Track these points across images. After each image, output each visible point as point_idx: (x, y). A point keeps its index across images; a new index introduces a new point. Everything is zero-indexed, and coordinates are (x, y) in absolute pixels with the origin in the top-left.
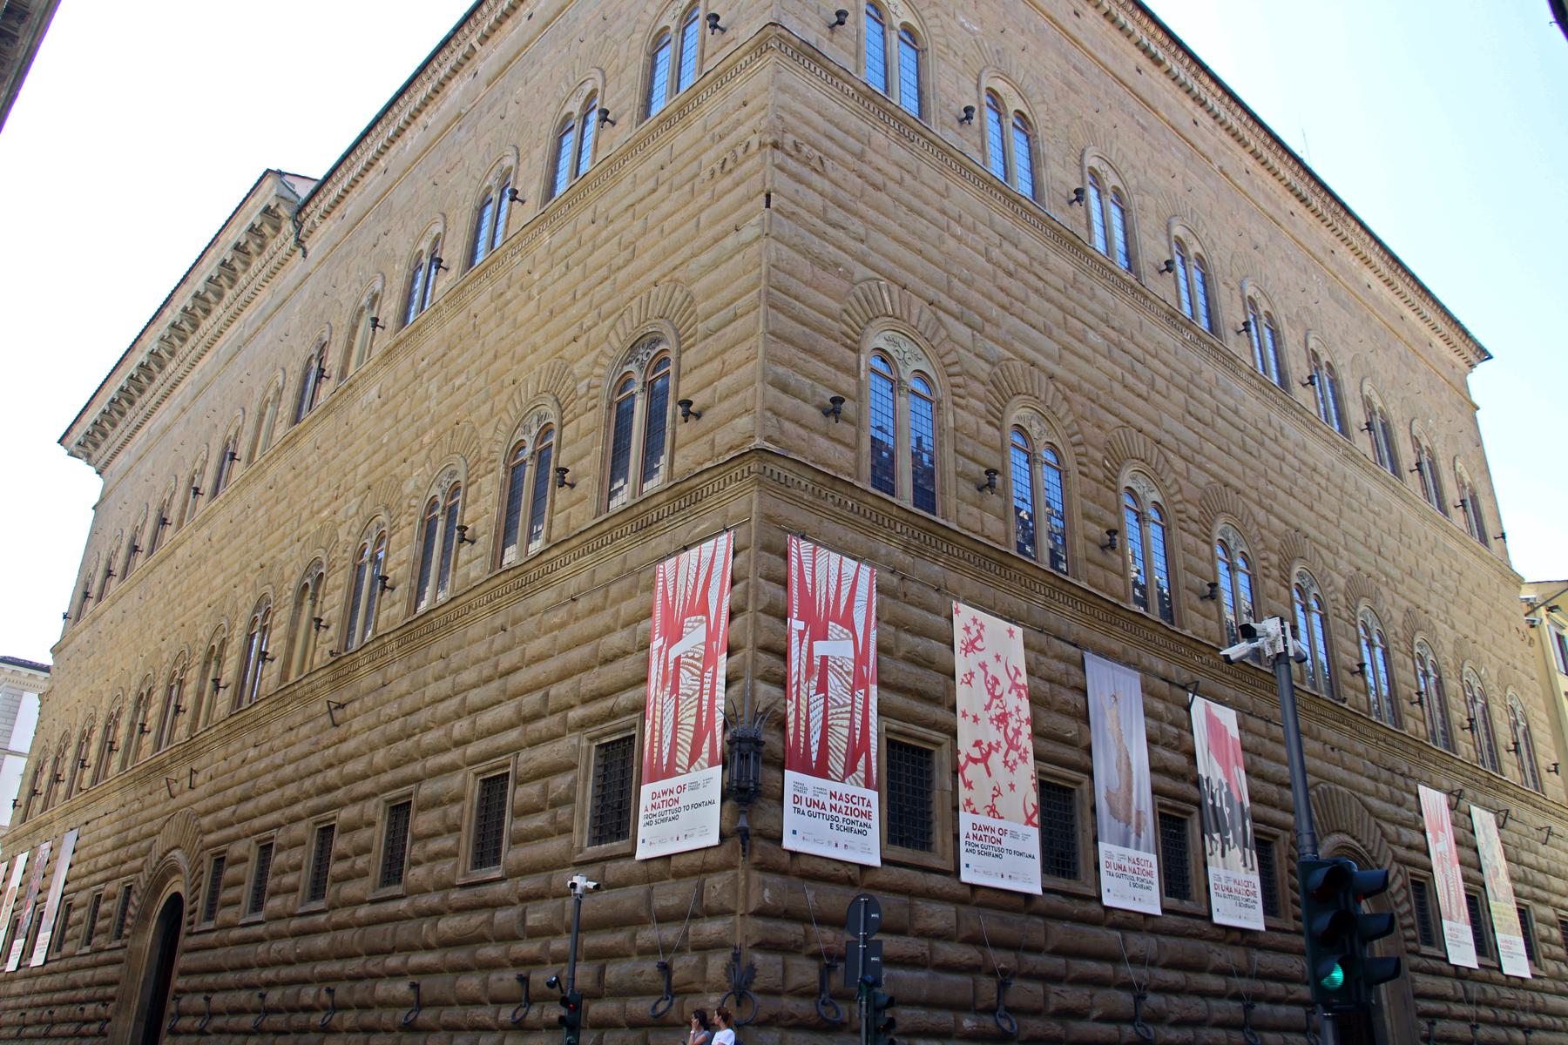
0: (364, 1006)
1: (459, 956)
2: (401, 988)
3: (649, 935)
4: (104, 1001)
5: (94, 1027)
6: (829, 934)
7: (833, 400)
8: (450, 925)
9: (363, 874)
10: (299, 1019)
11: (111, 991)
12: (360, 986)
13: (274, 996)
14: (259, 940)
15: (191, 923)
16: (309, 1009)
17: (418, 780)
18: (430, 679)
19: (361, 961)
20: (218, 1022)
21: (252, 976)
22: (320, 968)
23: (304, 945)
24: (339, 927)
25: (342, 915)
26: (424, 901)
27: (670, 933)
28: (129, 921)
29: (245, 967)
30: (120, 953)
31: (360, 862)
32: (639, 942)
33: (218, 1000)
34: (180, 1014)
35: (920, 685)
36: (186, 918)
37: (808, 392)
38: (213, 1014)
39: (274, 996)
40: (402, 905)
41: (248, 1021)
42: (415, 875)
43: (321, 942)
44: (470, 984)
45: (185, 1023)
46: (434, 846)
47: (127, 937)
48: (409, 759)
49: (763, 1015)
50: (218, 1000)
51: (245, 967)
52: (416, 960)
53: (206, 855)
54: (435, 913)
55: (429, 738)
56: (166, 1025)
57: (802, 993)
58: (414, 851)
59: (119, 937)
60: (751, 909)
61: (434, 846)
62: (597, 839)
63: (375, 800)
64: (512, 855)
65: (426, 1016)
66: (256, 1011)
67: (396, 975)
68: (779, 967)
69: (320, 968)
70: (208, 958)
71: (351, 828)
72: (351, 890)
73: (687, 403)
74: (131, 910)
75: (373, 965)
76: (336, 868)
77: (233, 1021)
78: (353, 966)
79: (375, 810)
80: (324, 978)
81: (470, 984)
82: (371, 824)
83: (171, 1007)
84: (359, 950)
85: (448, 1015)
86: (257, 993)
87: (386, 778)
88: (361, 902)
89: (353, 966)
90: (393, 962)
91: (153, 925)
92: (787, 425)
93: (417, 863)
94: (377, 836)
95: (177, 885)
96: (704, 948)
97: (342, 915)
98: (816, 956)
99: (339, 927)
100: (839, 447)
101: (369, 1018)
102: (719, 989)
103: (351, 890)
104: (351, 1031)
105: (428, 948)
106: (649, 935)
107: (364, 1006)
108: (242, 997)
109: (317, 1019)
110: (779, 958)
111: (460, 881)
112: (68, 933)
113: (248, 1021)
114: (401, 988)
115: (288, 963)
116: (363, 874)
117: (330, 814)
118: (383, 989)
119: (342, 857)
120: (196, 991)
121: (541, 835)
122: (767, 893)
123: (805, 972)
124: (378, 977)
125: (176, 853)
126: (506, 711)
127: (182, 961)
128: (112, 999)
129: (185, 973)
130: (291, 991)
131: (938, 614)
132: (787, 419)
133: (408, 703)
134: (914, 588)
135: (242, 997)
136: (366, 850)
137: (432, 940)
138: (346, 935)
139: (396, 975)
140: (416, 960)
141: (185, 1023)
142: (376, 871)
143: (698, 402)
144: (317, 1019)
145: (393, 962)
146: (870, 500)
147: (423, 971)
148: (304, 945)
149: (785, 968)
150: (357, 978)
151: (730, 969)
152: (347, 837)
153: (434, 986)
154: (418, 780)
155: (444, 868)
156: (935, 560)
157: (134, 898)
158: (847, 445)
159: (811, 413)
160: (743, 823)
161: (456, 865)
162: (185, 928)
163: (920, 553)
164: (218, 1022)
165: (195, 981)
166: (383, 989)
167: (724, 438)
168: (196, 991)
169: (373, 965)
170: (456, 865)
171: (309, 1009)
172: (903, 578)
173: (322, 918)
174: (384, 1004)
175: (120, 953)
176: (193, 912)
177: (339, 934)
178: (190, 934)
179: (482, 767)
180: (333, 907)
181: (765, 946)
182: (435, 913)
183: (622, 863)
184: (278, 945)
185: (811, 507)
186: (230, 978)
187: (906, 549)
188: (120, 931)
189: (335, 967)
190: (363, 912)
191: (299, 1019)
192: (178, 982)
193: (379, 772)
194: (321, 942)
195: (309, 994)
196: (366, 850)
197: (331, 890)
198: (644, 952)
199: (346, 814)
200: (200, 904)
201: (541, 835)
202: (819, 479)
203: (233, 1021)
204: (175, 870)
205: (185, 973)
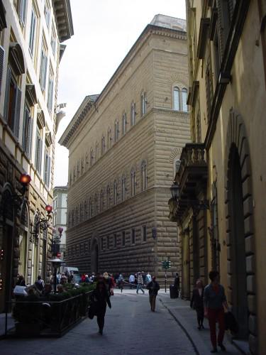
1: (131, 256)
13: (112, 262)
29: (107, 258)
42: (126, 244)
44: (133, 260)
54: (128, 250)
65: (129, 265)
70: (103, 256)
78: (121, 258)
90: (125, 257)
103: (119, 246)
114: (125, 261)
127: (100, 256)
136: (120, 240)
147: (128, 259)
192: (99, 260)
195: (116, 262)
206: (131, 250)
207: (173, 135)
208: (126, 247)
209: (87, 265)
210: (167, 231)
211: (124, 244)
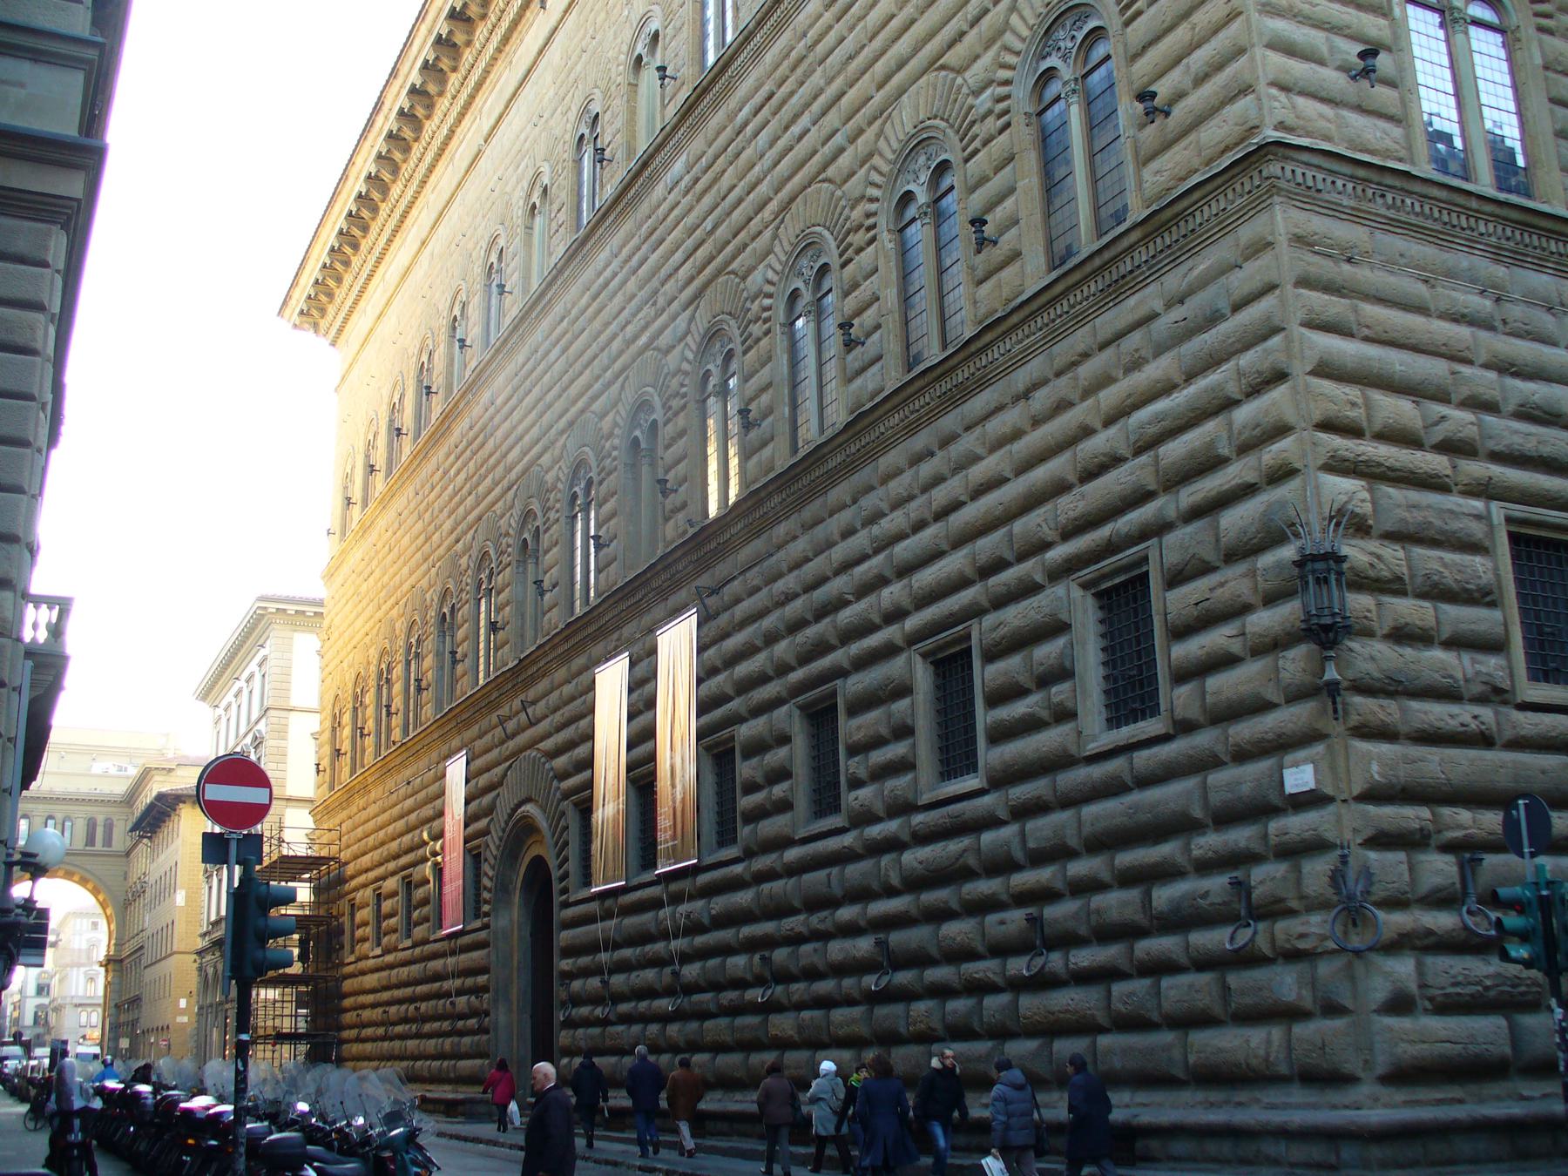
2: (864, 946)
3: (1209, 842)
6: (1464, 815)
7: (1363, 55)
8: (914, 858)
9: (784, 806)
11: (482, 979)
12: (806, 948)
15: (565, 891)
16: (740, 984)
17: (840, 673)
18: (836, 537)
19: (802, 917)
22: (747, 931)
23: (719, 904)
25: (763, 863)
26: (875, 831)
27: (1241, 836)
28: (486, 895)
30: (483, 935)
31: (779, 790)
32: (1196, 853)
35: (1546, 450)
36: (556, 887)
37: (1324, 50)
39: (691, 971)
40: (847, 840)
43: (743, 898)
44: (957, 930)
46: (879, 756)
47: (487, 914)
48: (821, 648)
49: (1387, 934)
52: (879, 908)
54: (893, 845)
55: (846, 616)
56: (560, 1016)
57: (1441, 900)
58: (850, 766)
59: (477, 916)
60: (1355, 793)
61: (879, 756)
62: (1114, 722)
63: (785, 708)
64: (990, 756)
67: (851, 930)
68: (1405, 867)
71: (756, 748)
72: (771, 827)
73: (1145, 96)
74: (486, 882)
75: (816, 920)
79: (787, 717)
81: (957, 930)
84: (797, 904)
86: (668, 970)
87: (796, 676)
90: (846, 913)
91: (517, 898)
92: (1301, 102)
93: (856, 784)
94: (797, 753)
96: (1294, 851)
97: (763, 863)
98: (1448, 848)
100: (1382, 124)
101: (825, 987)
102: (1323, 905)
103: (771, 827)
106: (1209, 842)
107: (812, 974)
108: (649, 975)
110: (1401, 856)
111: (925, 798)
112: (416, 915)
114: (864, 946)
116: (784, 806)
117: (725, 733)
118: (837, 949)
119: (751, 788)
121: (1030, 725)
122: (1375, 767)
123: (1439, 868)
124: (823, 936)
126: (954, 563)
127: (564, 937)
129: (569, 952)
130: (713, 963)
131: (1555, 344)
132: (1301, 93)
133: (810, 570)
134: (1516, 312)
136: (781, 774)
137: (895, 880)
138: (777, 886)
140: (879, 908)
142: (802, 803)
143: (1163, 88)
145: (846, 913)
146: (1435, 192)
148: (719, 904)
149: (1411, 869)
150: (795, 940)
151: (1337, 878)
152: (754, 761)
154: (840, 673)
155: (898, 784)
156: (1540, 267)
157: (486, 867)
158: (1390, 118)
159: (1332, 79)
160: (1331, 673)
161: (915, 780)
162: (558, 899)
163: (1517, 258)
165: (584, 961)
166: (837, 949)
167: (1214, 133)
169: (816, 920)
170: (915, 780)
172: (1498, 300)
174: (841, 970)
175: (483, 935)
176: (565, 876)
177: (766, 887)
178: (566, 905)
179: (929, 644)
180: (749, 854)
181: (1382, 840)
182: (893, 845)
183: (1155, 750)
184: (683, 908)
185: (1356, 216)
187: (1497, 255)
188: (478, 909)
189: (767, 927)
190: (792, 854)
191: (729, 996)
193: (783, 669)
194: (743, 898)
195: (738, 963)
196: (781, 774)
197: (744, 832)
198: (1205, 867)
201: (1030, 725)
202: (1361, 173)
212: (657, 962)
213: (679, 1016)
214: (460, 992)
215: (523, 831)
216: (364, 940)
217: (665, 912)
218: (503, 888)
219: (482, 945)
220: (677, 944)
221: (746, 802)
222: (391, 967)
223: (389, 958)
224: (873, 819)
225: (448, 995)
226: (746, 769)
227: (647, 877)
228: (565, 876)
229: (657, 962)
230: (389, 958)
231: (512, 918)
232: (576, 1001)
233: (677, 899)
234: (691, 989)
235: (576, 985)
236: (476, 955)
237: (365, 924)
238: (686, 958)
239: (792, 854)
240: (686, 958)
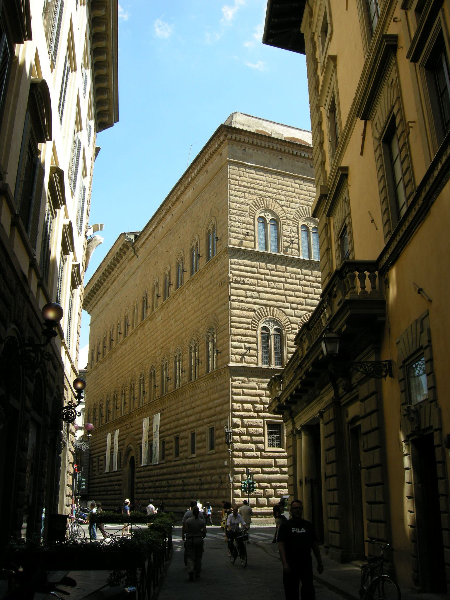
0: (175, 486)
2: (180, 482)
4: (120, 485)
5: (118, 492)
9: (171, 454)
10: (163, 489)
11: (121, 482)
12: (173, 481)
13: (157, 484)
14: (152, 470)
16: (165, 487)
20: (146, 490)
21: (151, 479)
22: (166, 477)
24: (168, 467)
25: (168, 464)
28: (122, 463)
29: (150, 476)
30: (121, 472)
31: (171, 451)
33: (146, 485)
34: (138, 488)
36: (136, 464)
38: (145, 488)
39: (157, 484)
41: (152, 490)
42: (181, 455)
43: (165, 471)
45: (139, 491)
50: (146, 485)
51: (150, 476)
53: (138, 446)
56: (135, 491)
65: (185, 488)
66: (154, 487)
67: (180, 478)
69: (166, 477)
70: (142, 474)
74: (122, 460)
76: (166, 452)
77: (149, 490)
78: (172, 476)
80: (167, 480)
82: (172, 442)
83: (135, 487)
85: (190, 487)
88: (172, 461)
89: (172, 476)
90: (179, 475)
93: (181, 452)
95: (132, 454)
97: (168, 464)
99: (168, 467)
101: (176, 488)
103: (170, 458)
104: (173, 492)
105: (185, 472)
107: (175, 486)
109: (166, 489)
113: (152, 490)
114: (180, 482)
115: (160, 476)
116: (171, 454)
119: (167, 450)
120: (140, 482)
125: (131, 445)
127: (137, 475)
128: (121, 485)
129: (138, 478)
130: (160, 482)
135: (150, 484)
136: (171, 448)
138: (169, 469)
139: (180, 478)
141: (139, 491)
144: (166, 489)
145: (179, 475)
147: (185, 478)
150: (173, 479)
153: (186, 481)
162: (136, 466)
164: (146, 490)
165: (140, 480)
168: (140, 482)
171: (165, 487)
173: (164, 465)
175: (121, 472)
176: (137, 462)
178: (137, 468)
180: (166, 462)
186: (147, 479)
189: (168, 476)
190: (172, 463)
191: (163, 489)
192: (136, 480)
194: (165, 471)
195: (164, 483)
199: (167, 439)
200: (138, 460)
203: (149, 490)
204: (131, 450)
205: (138, 478)
206: (190, 464)
207: (257, 288)
208: (182, 459)
209: (117, 487)
210: (249, 434)
211: (177, 455)
212: (152, 481)
213: (154, 492)
214: (116, 485)
215: (129, 450)
216: (95, 471)
217: (153, 472)
218: (125, 462)
219: (121, 475)
220: (155, 478)
221: (166, 452)
222: (101, 478)
223: (101, 476)
224: (183, 459)
225: (113, 485)
226: (166, 446)
227: (150, 464)
228: (137, 462)
229: (152, 481)
230: (101, 476)
231: (127, 469)
232: (138, 488)
233: (155, 469)
234: (157, 487)
235: (138, 485)
236: (120, 477)
237: (95, 467)
238: (156, 481)
239: (172, 463)
240: (156, 481)
